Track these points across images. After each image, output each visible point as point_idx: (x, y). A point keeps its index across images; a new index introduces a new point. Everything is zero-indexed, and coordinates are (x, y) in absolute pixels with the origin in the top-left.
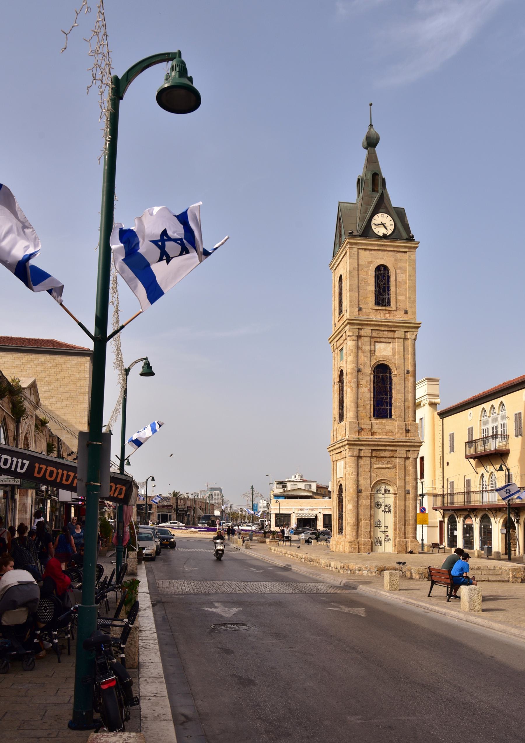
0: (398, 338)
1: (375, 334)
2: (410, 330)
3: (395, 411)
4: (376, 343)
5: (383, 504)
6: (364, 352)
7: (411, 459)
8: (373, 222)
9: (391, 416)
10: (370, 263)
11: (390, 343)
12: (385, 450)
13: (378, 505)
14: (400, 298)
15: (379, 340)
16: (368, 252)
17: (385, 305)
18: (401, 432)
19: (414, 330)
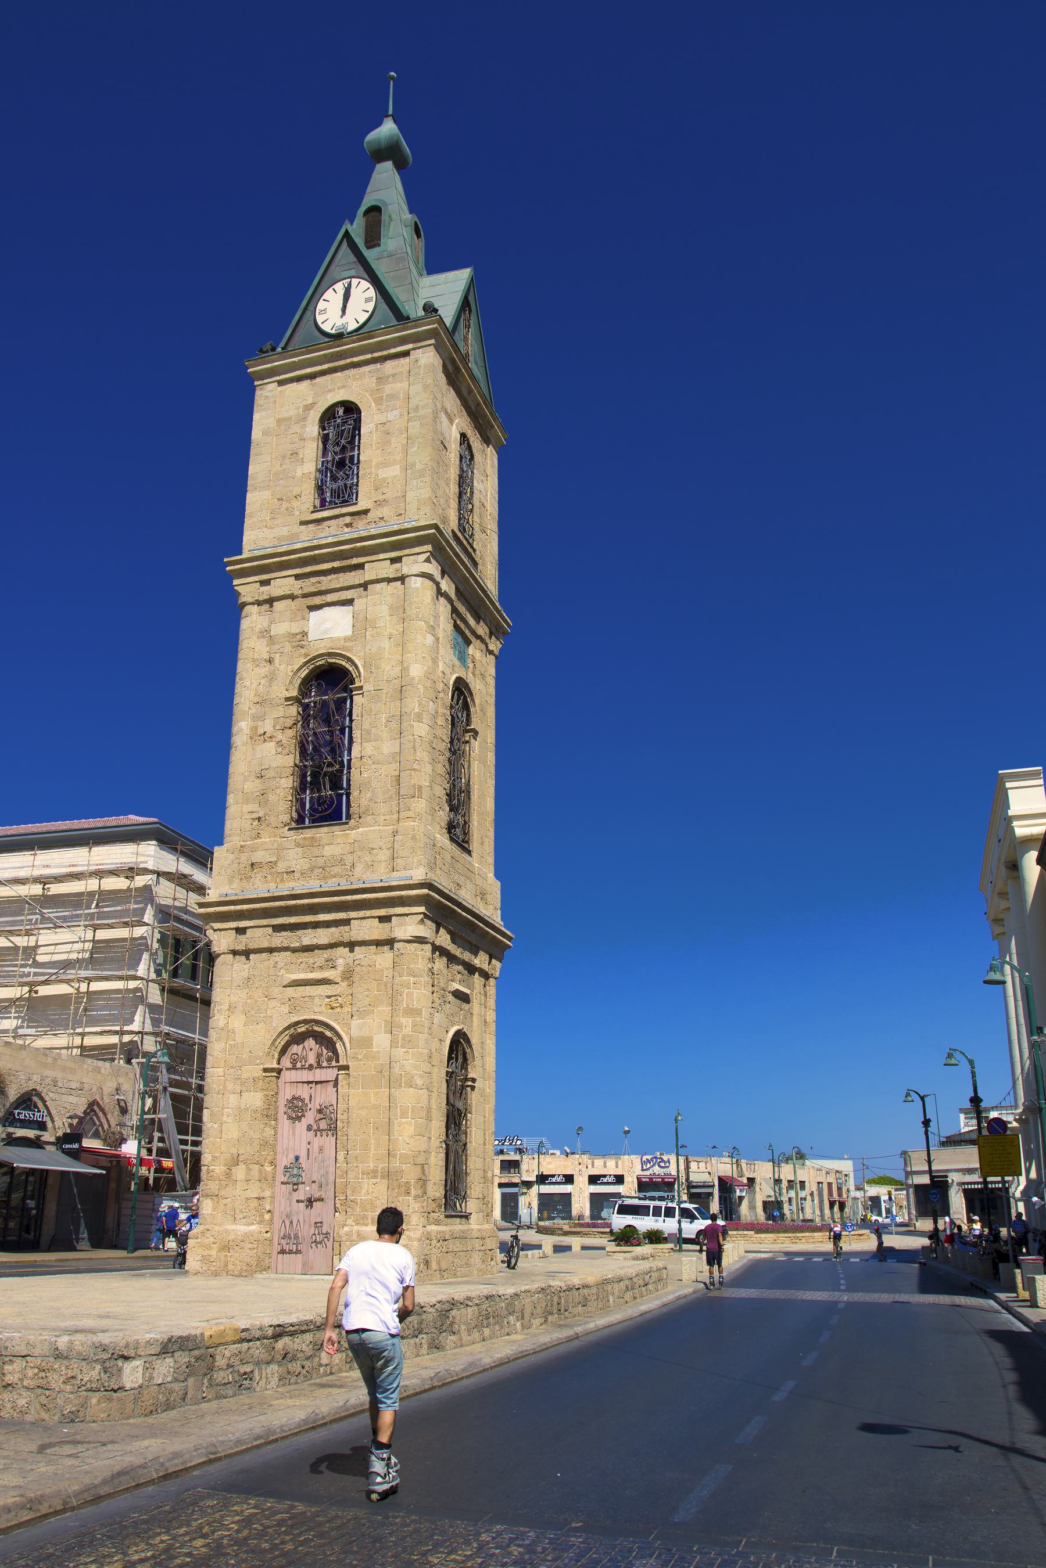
0: (373, 582)
1: (309, 585)
2: (407, 552)
3: (359, 799)
4: (313, 615)
5: (309, 1106)
6: (272, 640)
7: (396, 945)
8: (321, 305)
9: (349, 817)
10: (308, 408)
11: (350, 602)
12: (316, 925)
13: (296, 1109)
14: (383, 473)
15: (317, 600)
16: (306, 383)
17: (343, 502)
18: (368, 858)
19: (417, 550)
